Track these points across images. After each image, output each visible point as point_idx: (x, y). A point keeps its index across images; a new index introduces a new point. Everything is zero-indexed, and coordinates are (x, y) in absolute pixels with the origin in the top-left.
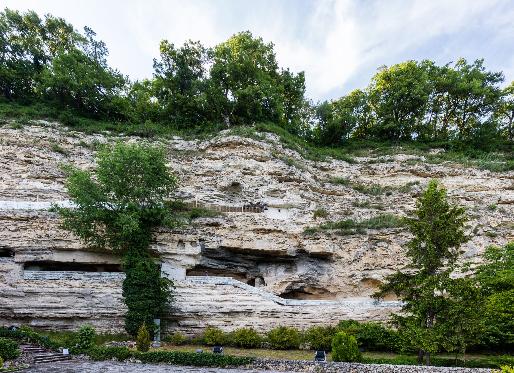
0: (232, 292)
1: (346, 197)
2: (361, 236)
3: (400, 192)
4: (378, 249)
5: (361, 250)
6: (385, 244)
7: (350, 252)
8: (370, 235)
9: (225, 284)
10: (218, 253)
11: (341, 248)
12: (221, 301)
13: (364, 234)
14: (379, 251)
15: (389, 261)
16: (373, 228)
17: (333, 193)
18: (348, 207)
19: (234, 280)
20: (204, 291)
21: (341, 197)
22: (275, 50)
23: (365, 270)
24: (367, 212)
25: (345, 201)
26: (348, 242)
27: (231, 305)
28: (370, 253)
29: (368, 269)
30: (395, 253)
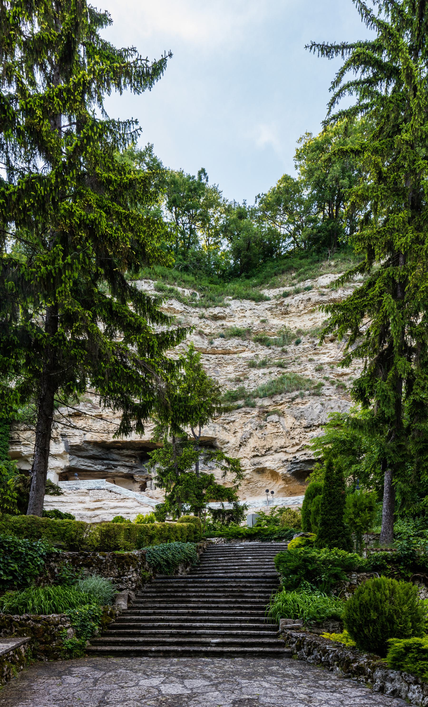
0: (104, 498)
1: (243, 355)
2: (248, 409)
3: (311, 337)
4: (269, 425)
5: (247, 429)
6: (275, 418)
7: (236, 434)
8: (261, 407)
9: (99, 489)
10: (87, 450)
11: (225, 429)
12: (93, 510)
13: (253, 406)
14: (270, 429)
15: (280, 442)
16: (265, 396)
17: (227, 352)
18: (242, 369)
19: (107, 483)
20: (76, 498)
21: (235, 356)
22: (156, 152)
23: (254, 456)
24: (264, 374)
25: (241, 362)
26: (233, 419)
27: (103, 514)
28: (258, 433)
29: (257, 456)
30: (289, 429)
